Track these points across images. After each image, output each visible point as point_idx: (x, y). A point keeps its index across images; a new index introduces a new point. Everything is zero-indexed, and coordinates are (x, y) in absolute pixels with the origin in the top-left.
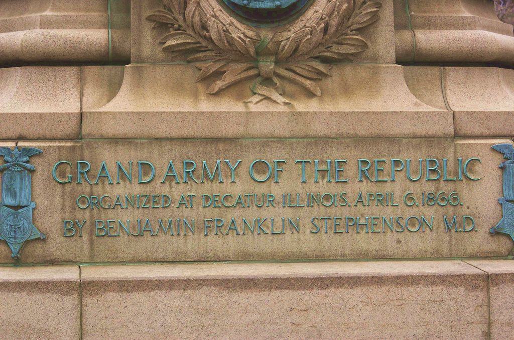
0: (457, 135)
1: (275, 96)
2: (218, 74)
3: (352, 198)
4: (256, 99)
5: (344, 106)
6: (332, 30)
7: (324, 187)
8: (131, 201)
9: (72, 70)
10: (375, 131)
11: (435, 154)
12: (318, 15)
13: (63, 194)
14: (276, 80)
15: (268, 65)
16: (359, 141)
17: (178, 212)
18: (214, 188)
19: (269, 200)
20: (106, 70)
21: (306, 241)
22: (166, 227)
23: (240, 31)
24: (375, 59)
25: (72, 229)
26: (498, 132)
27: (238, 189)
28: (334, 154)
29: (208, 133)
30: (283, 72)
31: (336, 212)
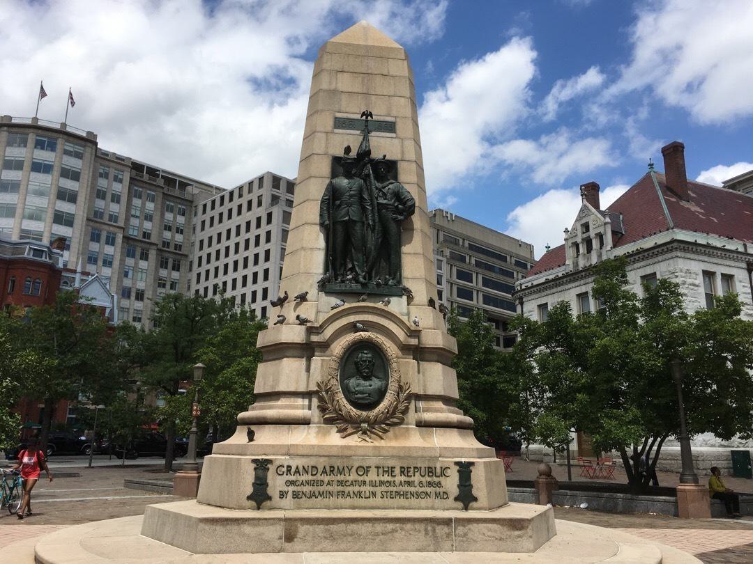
1: (368, 439)
5: (394, 444)
7: (386, 478)
8: (307, 482)
14: (368, 432)
17: (327, 488)
18: (340, 477)
19: (364, 483)
22: (321, 494)
23: (354, 412)
28: (391, 463)
31: (391, 489)
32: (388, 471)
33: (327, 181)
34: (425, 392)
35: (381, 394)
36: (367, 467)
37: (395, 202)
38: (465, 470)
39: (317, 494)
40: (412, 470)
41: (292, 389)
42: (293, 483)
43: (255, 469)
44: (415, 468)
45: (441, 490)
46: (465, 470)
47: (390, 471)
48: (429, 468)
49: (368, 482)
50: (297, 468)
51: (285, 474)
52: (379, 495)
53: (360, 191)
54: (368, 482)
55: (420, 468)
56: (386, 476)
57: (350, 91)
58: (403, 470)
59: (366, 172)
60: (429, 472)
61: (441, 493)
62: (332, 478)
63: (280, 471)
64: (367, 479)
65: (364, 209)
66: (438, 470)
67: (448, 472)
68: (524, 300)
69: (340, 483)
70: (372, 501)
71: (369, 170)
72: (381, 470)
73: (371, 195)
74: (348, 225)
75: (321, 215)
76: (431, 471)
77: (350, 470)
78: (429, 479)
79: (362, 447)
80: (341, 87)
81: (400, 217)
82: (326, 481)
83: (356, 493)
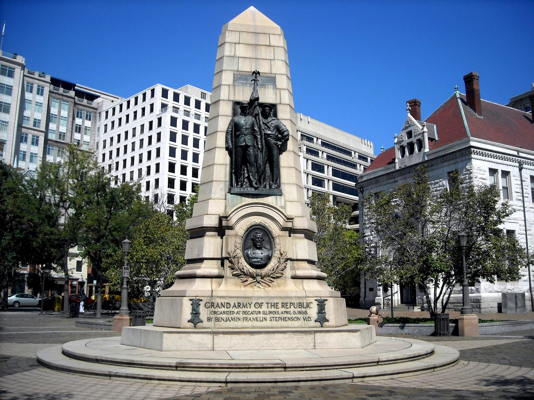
1: (261, 286)
2: (247, 281)
4: (256, 287)
7: (273, 309)
9: (209, 279)
10: (286, 295)
11: (301, 301)
13: (207, 311)
14: (260, 282)
15: (259, 278)
16: (282, 298)
18: (245, 309)
21: (268, 323)
23: (252, 270)
24: (285, 277)
25: (209, 319)
27: (251, 310)
28: (275, 301)
29: (244, 296)
30: (262, 280)
31: (275, 316)
33: (230, 118)
34: (296, 257)
35: (269, 258)
37: (276, 132)
38: (321, 304)
39: (230, 319)
40: (289, 304)
41: (211, 256)
42: (215, 313)
43: (192, 305)
44: (290, 303)
46: (321, 304)
47: (275, 305)
49: (261, 312)
51: (210, 307)
52: (268, 319)
53: (253, 126)
54: (261, 312)
57: (244, 56)
58: (283, 304)
59: (256, 112)
61: (307, 318)
62: (240, 309)
63: (207, 306)
64: (261, 310)
65: (255, 137)
66: (305, 305)
67: (311, 305)
68: (364, 189)
69: (244, 313)
70: (264, 323)
71: (258, 110)
72: (269, 305)
73: (260, 128)
75: (227, 142)
76: (301, 305)
77: (250, 305)
78: (299, 310)
80: (238, 54)
82: (236, 312)
83: (254, 318)
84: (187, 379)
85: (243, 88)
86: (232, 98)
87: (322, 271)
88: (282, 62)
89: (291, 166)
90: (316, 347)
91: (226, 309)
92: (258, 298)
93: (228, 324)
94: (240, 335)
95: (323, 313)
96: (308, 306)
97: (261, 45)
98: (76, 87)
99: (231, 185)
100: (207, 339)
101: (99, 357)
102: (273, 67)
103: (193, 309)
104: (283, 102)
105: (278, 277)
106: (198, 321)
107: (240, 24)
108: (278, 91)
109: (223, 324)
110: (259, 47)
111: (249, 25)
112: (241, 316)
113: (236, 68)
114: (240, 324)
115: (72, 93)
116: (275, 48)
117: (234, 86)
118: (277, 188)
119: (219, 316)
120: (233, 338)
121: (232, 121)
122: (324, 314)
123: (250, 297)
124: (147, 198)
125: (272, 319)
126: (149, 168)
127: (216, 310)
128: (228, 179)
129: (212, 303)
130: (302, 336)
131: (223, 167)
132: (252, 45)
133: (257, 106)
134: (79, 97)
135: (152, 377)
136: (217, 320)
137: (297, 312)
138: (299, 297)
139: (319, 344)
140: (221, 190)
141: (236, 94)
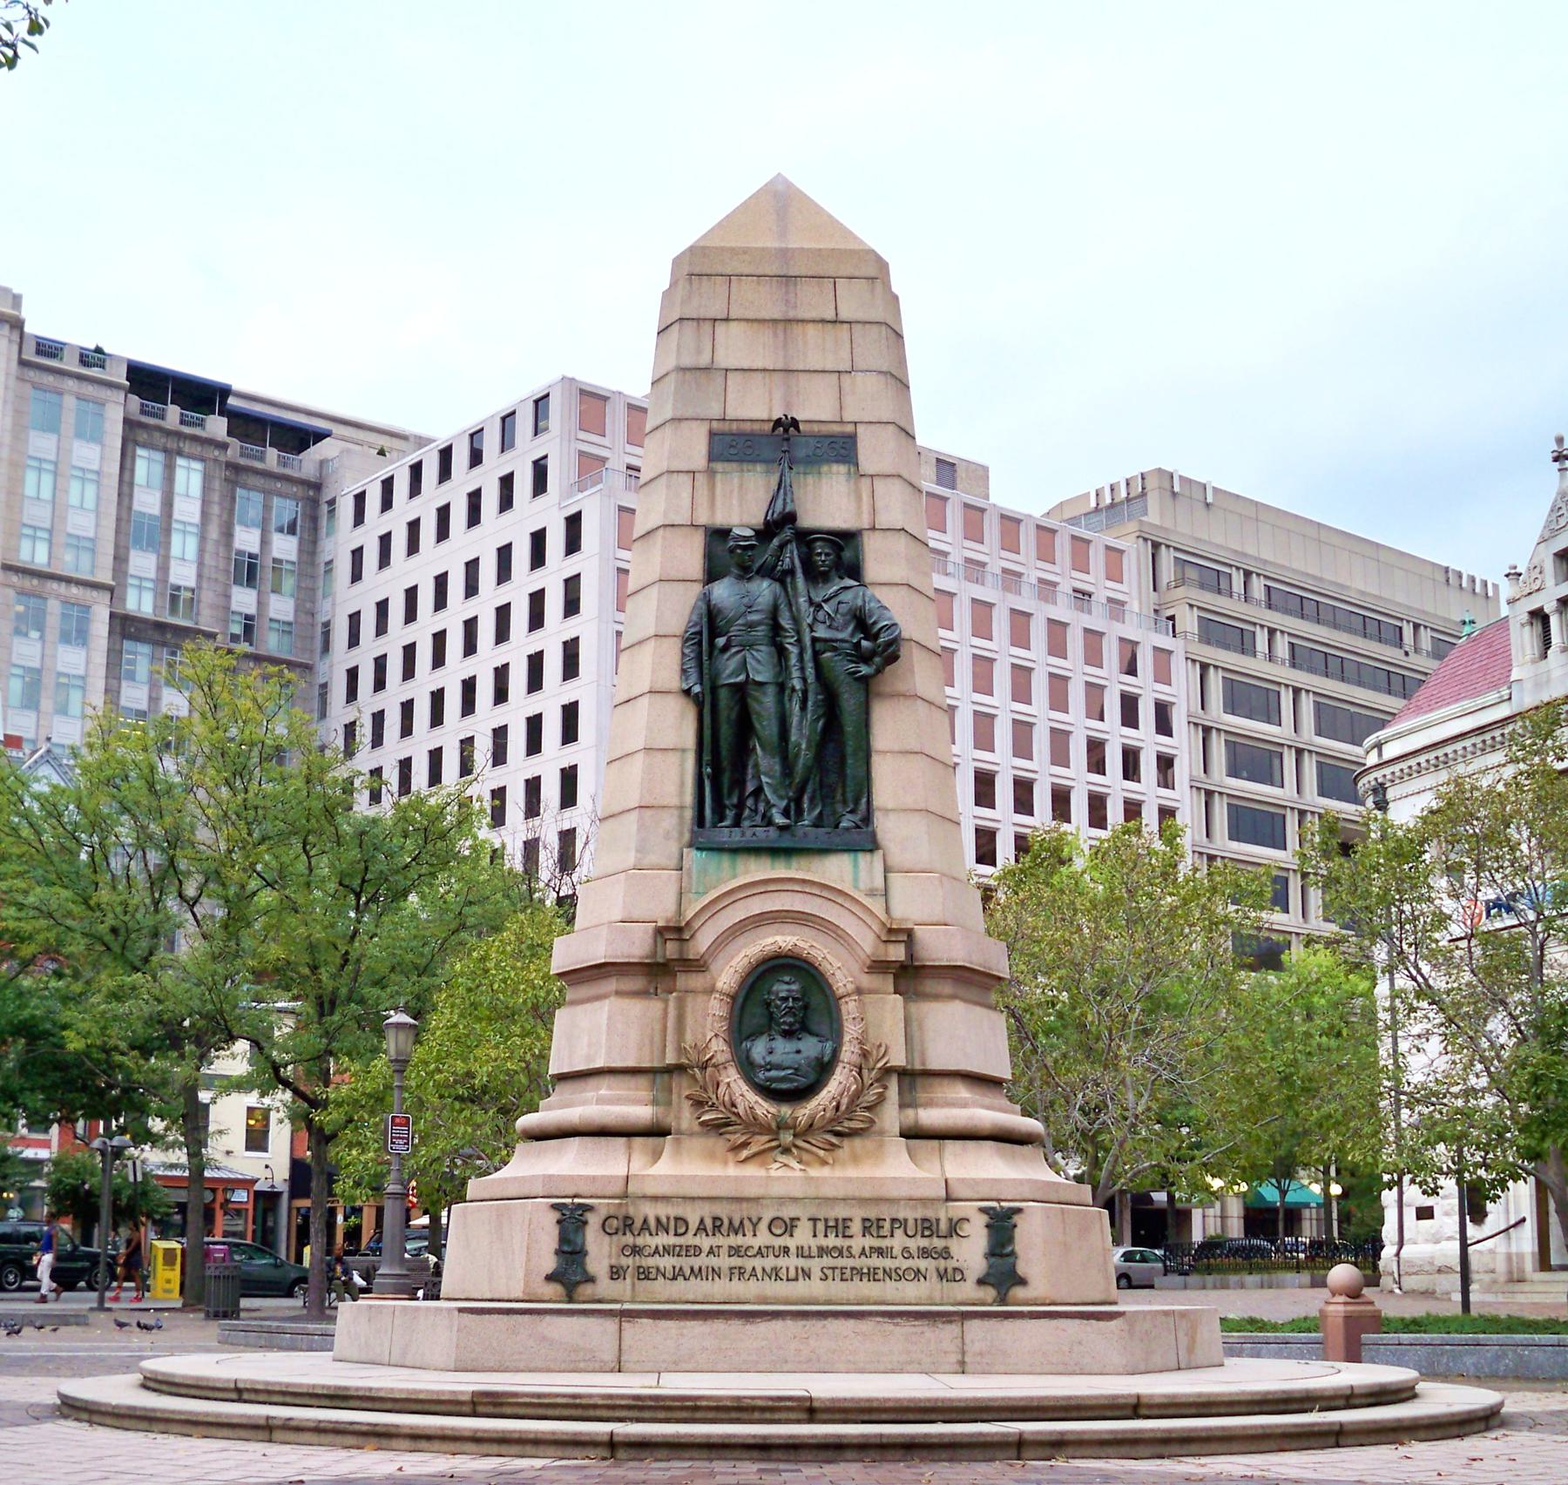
0: (948, 1199)
2: (745, 1145)
3: (856, 1251)
4: (778, 1165)
5: (852, 1172)
6: (843, 1108)
7: (832, 1241)
9: (623, 1140)
11: (930, 1214)
12: (831, 1095)
15: (787, 1138)
16: (863, 1201)
20: (651, 1141)
22: (697, 1273)
23: (764, 1108)
24: (882, 1133)
25: (616, 1273)
26: (986, 1196)
27: (757, 1242)
28: (841, 1212)
30: (800, 1143)
31: (841, 1262)
32: (836, 1227)
33: (697, 589)
35: (824, 1069)
36: (792, 1219)
37: (852, 635)
38: (1002, 1224)
39: (687, 1272)
40: (887, 1225)
41: (631, 1063)
42: (636, 1250)
43: (559, 1222)
44: (894, 1220)
45: (951, 1264)
46: (1002, 1224)
47: (840, 1227)
48: (925, 1220)
49: (793, 1250)
50: (645, 1221)
51: (620, 1233)
52: (816, 1273)
53: (774, 613)
54: (793, 1250)
55: (906, 1220)
56: (832, 1236)
58: (868, 1224)
60: (924, 1228)
61: (950, 1270)
63: (610, 1227)
64: (791, 1243)
65: (781, 652)
66: (943, 1226)
67: (966, 1229)
68: (1390, 795)
69: (735, 1251)
70: (801, 1288)
71: (792, 557)
72: (821, 1226)
73: (796, 620)
74: (741, 691)
76: (927, 1227)
78: (924, 1243)
79: (779, 1178)
80: (725, 359)
81: (865, 670)
82: (706, 1248)
83: (768, 1270)
84: (494, 1435)
85: (741, 478)
86: (703, 518)
87: (1025, 1113)
88: (882, 378)
89: (908, 748)
90: (968, 1368)
91: (671, 1240)
92: (782, 1200)
93: (680, 1288)
94: (709, 1322)
95: (1008, 1255)
96: (954, 1229)
97: (803, 321)
98: (231, 401)
99: (700, 820)
100: (599, 1333)
101: (245, 1381)
102: (848, 400)
103: (563, 1239)
104: (883, 520)
105: (853, 1133)
106: (578, 1278)
107: (732, 250)
108: (865, 483)
109: (661, 1288)
110: (798, 329)
111: (763, 249)
112: (724, 1262)
113: (715, 411)
114: (719, 1289)
115: (217, 426)
116: (857, 328)
117: (711, 473)
118: (858, 827)
119: (651, 1262)
120: (685, 1331)
121: (706, 598)
122: (1011, 1260)
123: (757, 1200)
124: (496, 855)
125: (829, 1272)
126: (500, 734)
127: (640, 1241)
128: (689, 798)
129: (627, 1218)
130: (919, 1330)
131: (673, 758)
132: (775, 321)
133: (789, 541)
134: (243, 437)
135: (393, 1430)
136: (644, 1274)
137: (914, 1252)
138: (924, 1201)
139: (978, 1359)
140: (667, 836)
141: (719, 503)
